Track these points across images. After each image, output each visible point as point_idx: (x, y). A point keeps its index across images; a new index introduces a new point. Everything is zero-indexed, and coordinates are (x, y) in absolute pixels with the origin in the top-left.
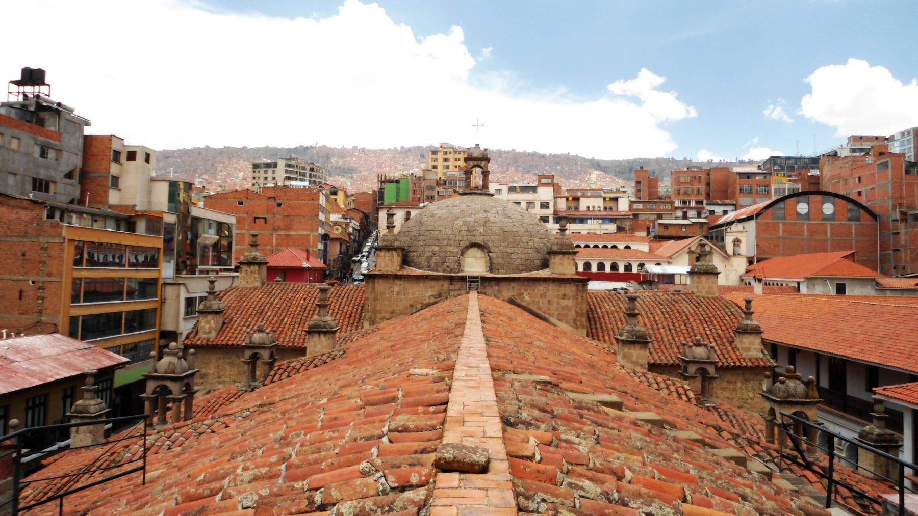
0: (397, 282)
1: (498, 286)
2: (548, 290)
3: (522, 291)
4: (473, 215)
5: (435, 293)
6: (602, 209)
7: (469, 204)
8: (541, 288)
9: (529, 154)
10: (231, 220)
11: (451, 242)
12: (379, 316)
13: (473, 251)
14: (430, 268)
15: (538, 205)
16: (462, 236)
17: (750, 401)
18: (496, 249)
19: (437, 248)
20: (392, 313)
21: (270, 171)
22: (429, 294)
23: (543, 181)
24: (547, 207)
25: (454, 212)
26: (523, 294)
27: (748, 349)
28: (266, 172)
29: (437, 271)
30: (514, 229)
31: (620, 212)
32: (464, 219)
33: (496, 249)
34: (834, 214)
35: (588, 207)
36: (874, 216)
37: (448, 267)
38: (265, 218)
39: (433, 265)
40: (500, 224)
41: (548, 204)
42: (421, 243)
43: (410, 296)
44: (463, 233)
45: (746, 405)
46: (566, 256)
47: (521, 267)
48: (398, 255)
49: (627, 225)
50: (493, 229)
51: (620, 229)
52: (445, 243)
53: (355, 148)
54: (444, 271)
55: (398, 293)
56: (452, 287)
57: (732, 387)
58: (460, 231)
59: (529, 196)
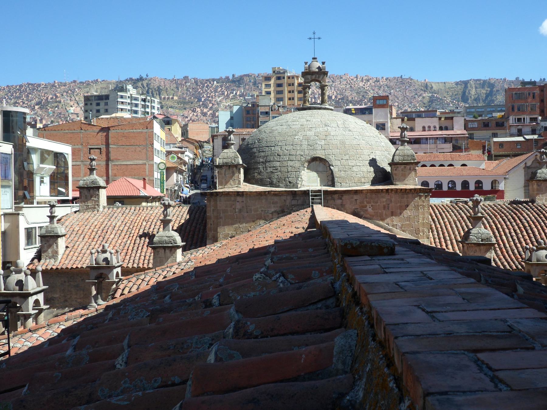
0: (239, 199)
1: (341, 199)
2: (391, 201)
3: (365, 203)
4: (313, 129)
5: (278, 209)
7: (308, 118)
8: (384, 200)
10: (66, 149)
11: (291, 158)
14: (271, 184)
16: (303, 150)
18: (338, 163)
19: (278, 164)
21: (102, 103)
22: (273, 210)
23: (378, 102)
25: (294, 127)
26: (366, 206)
28: (98, 104)
29: (278, 187)
30: (355, 142)
32: (305, 133)
33: (338, 163)
37: (290, 182)
38: (100, 149)
39: (275, 181)
40: (339, 138)
42: (261, 160)
43: (253, 213)
44: (305, 147)
47: (363, 180)
49: (463, 144)
50: (333, 142)
52: (286, 158)
53: (186, 78)
54: (286, 186)
55: (240, 211)
56: (294, 202)
58: (301, 145)
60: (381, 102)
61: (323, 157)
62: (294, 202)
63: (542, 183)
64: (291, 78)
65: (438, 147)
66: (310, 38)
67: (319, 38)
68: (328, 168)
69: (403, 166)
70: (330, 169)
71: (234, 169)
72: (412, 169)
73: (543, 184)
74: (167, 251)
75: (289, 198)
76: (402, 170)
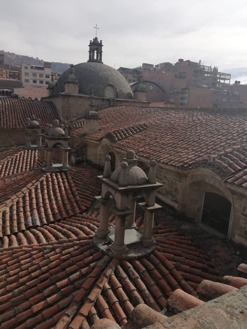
0: (80, 99)
9: (10, 54)
12: (72, 115)
13: (108, 88)
15: (44, 76)
20: (77, 114)
24: (49, 78)
34: (152, 90)
36: (163, 91)
37: (100, 94)
41: (49, 76)
46: (143, 93)
48: (78, 87)
50: (116, 79)
54: (99, 96)
55: (80, 105)
56: (103, 103)
59: (41, 71)
61: (113, 85)
62: (103, 103)
68: (115, 90)
69: (141, 93)
70: (116, 90)
71: (76, 85)
74: (95, 120)
75: (101, 101)
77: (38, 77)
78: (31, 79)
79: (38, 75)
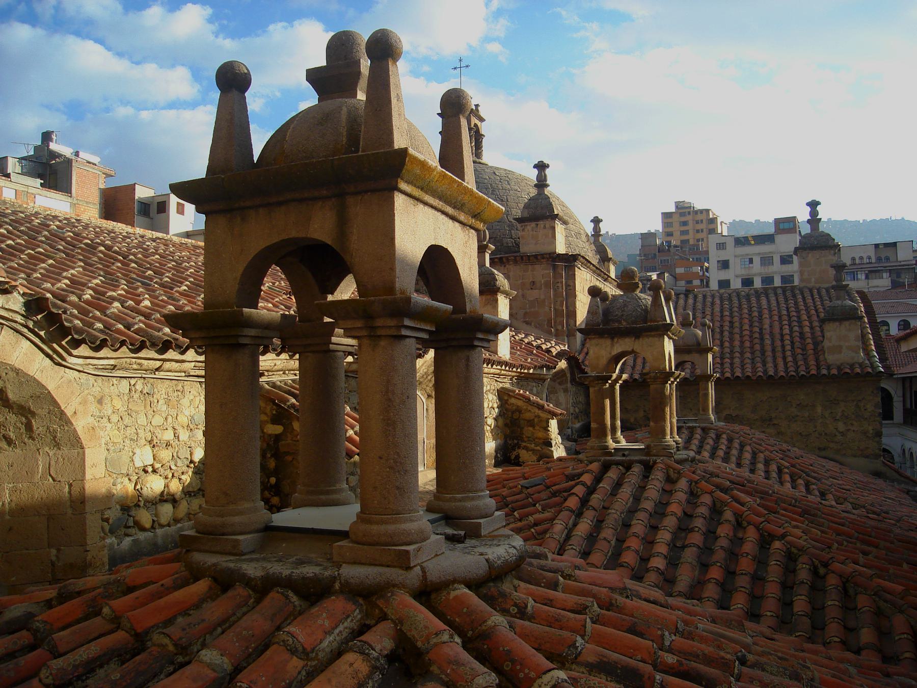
6: (873, 260)
15: (777, 260)
17: (839, 437)
27: (838, 349)
31: (900, 262)
35: (853, 259)
45: (832, 445)
46: (541, 223)
51: (895, 285)
57: (807, 414)
59: (766, 248)
60: (786, 226)
63: (808, 253)
64: (699, 213)
65: (870, 285)
66: (455, 68)
67: (467, 66)
69: (533, 224)
72: (547, 226)
73: (810, 255)
76: (532, 230)
77: (757, 267)
78: (737, 276)
79: (757, 260)
